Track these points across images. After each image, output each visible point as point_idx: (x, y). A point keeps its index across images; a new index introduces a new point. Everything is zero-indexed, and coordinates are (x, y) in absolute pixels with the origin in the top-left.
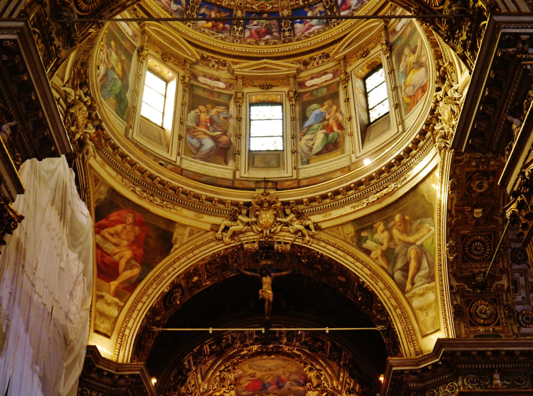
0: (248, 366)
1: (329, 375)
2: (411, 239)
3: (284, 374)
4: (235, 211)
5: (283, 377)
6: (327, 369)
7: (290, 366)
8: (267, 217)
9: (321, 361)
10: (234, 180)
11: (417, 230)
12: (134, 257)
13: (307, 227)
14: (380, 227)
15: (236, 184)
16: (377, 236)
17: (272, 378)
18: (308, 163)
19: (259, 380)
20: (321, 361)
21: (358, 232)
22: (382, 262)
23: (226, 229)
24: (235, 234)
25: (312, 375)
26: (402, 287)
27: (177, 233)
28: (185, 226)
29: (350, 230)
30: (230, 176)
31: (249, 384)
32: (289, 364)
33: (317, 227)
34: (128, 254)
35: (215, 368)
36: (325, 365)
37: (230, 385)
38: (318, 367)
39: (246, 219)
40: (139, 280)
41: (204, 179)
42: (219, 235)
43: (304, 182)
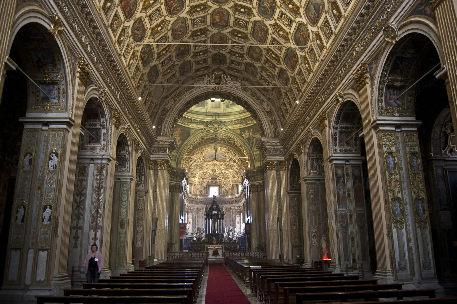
2: (255, 136)
4: (207, 124)
8: (216, 126)
10: (206, 113)
11: (256, 135)
12: (180, 139)
13: (227, 129)
14: (247, 131)
15: (207, 114)
16: (246, 134)
18: (228, 107)
21: (241, 132)
22: (247, 141)
23: (205, 129)
24: (207, 131)
25: (228, 156)
26: (251, 148)
27: (192, 131)
28: (193, 129)
29: (239, 131)
30: (205, 111)
33: (230, 129)
34: (179, 138)
39: (210, 126)
40: (182, 145)
41: (198, 113)
42: (203, 131)
43: (227, 114)
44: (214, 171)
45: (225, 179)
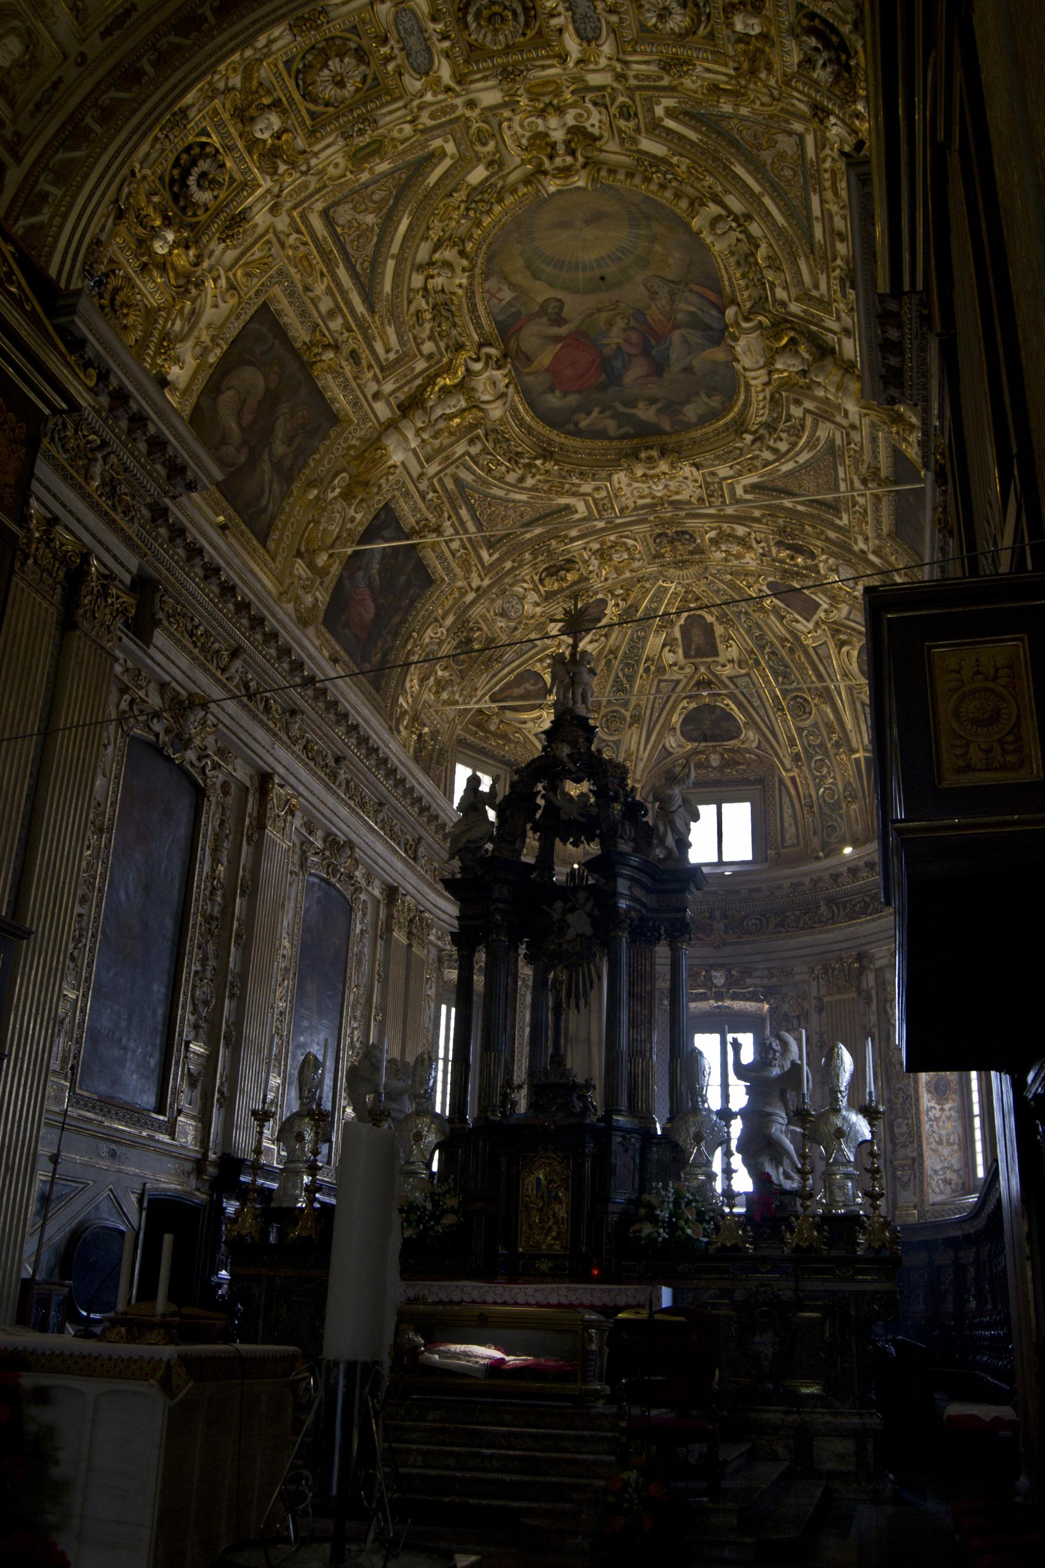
0: (520, 262)
1: (780, 232)
3: (654, 295)
5: (654, 313)
6: (767, 200)
7: (658, 248)
9: (739, 170)
17: (620, 323)
19: (581, 338)
20: (739, 170)
31: (556, 357)
32: (653, 239)
35: (395, 249)
36: (757, 188)
37: (481, 345)
38: (735, 204)
44: (698, 638)
45: (801, 708)
